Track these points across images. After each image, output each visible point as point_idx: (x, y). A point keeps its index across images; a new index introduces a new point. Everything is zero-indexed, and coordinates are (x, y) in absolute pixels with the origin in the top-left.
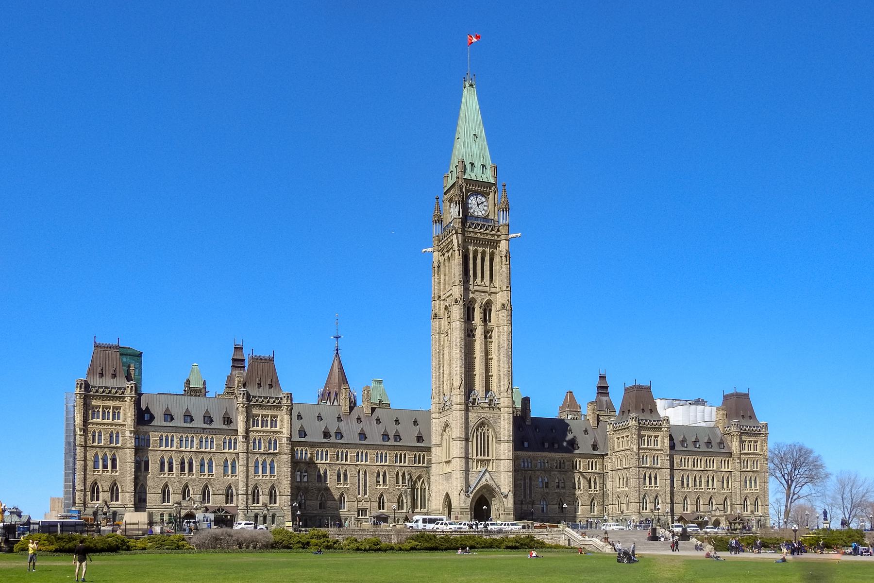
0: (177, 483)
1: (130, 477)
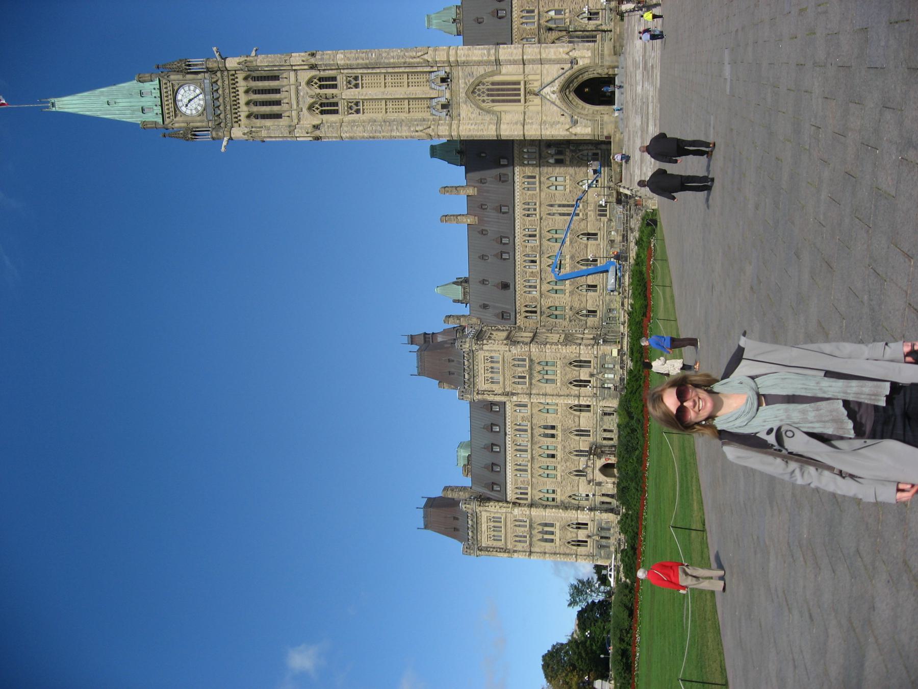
0: (568, 464)
1: (561, 513)
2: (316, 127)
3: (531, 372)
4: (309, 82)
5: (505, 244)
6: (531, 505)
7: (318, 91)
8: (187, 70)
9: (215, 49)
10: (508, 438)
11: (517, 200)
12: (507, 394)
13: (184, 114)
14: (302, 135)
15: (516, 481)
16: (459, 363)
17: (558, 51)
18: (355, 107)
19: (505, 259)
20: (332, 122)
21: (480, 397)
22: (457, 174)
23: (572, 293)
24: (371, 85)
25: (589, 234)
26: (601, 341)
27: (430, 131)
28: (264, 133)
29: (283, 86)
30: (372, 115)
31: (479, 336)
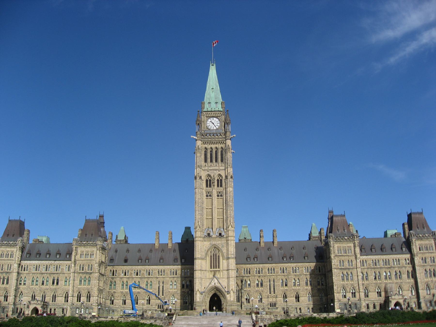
0: (39, 291)
1: (13, 288)
2: (200, 178)
3: (85, 274)
4: (220, 175)
5: (146, 261)
6: (18, 273)
7: (216, 179)
8: (226, 123)
9: (235, 135)
10: (53, 262)
11: (166, 267)
13: (207, 121)
14: (197, 171)
15: (31, 265)
16: (91, 239)
17: (233, 286)
18: (209, 195)
19: (138, 261)
20: (202, 185)
21: (74, 249)
22: (178, 239)
23: (122, 292)
24: (218, 202)
25: (149, 300)
26: (99, 307)
27: (198, 228)
28: (198, 155)
29: (218, 164)
30: (205, 202)
31: (103, 249)
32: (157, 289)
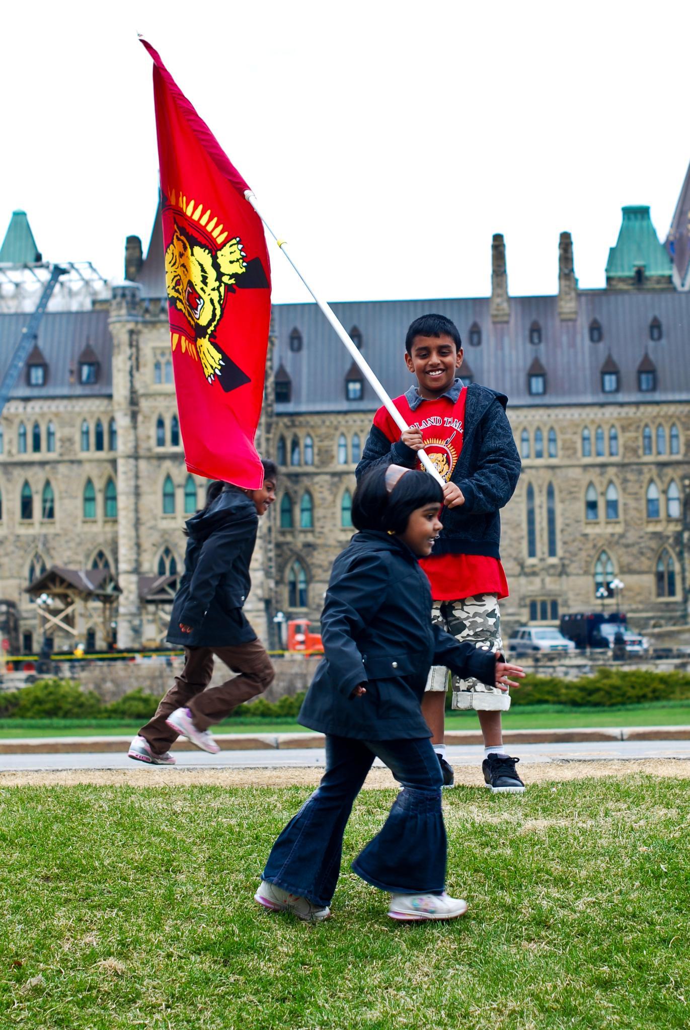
12: (133, 400)
32: (524, 526)
